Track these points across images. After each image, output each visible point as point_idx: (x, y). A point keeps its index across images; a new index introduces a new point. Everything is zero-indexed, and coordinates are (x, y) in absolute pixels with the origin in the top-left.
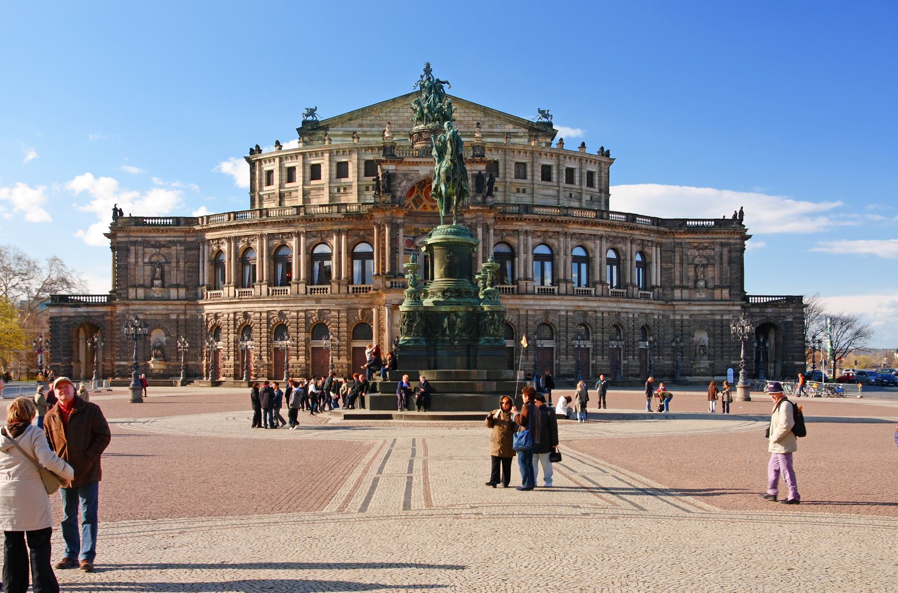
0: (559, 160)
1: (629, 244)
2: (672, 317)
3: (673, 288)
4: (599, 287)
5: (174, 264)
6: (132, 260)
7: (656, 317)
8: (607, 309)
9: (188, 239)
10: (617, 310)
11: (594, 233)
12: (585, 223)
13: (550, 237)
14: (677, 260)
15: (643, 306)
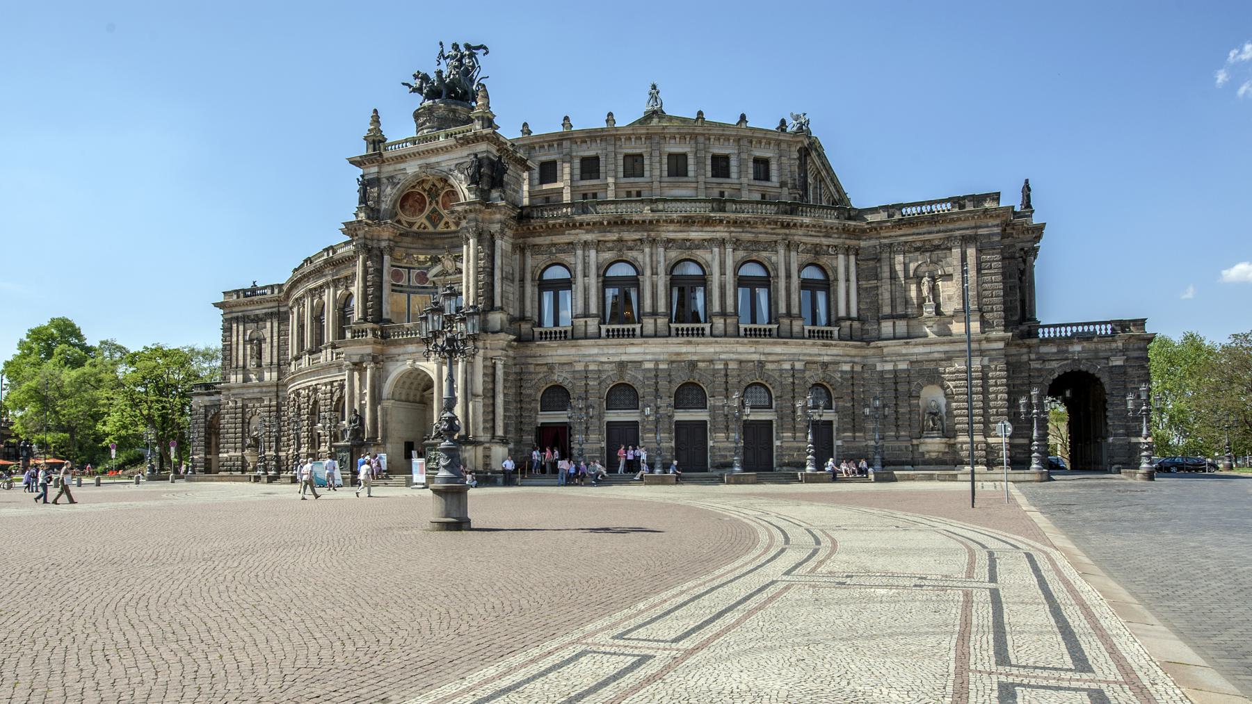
0: (696, 143)
1: (782, 252)
2: (879, 368)
3: (879, 319)
4: (719, 323)
5: (268, 340)
6: (234, 339)
7: (847, 368)
8: (734, 357)
9: (282, 309)
10: (756, 357)
11: (707, 236)
12: (688, 222)
13: (631, 249)
14: (886, 274)
15: (815, 350)
